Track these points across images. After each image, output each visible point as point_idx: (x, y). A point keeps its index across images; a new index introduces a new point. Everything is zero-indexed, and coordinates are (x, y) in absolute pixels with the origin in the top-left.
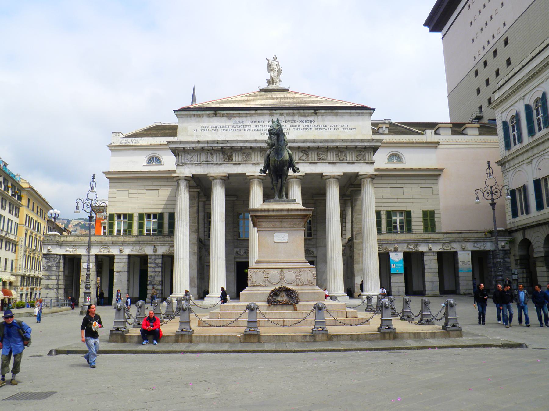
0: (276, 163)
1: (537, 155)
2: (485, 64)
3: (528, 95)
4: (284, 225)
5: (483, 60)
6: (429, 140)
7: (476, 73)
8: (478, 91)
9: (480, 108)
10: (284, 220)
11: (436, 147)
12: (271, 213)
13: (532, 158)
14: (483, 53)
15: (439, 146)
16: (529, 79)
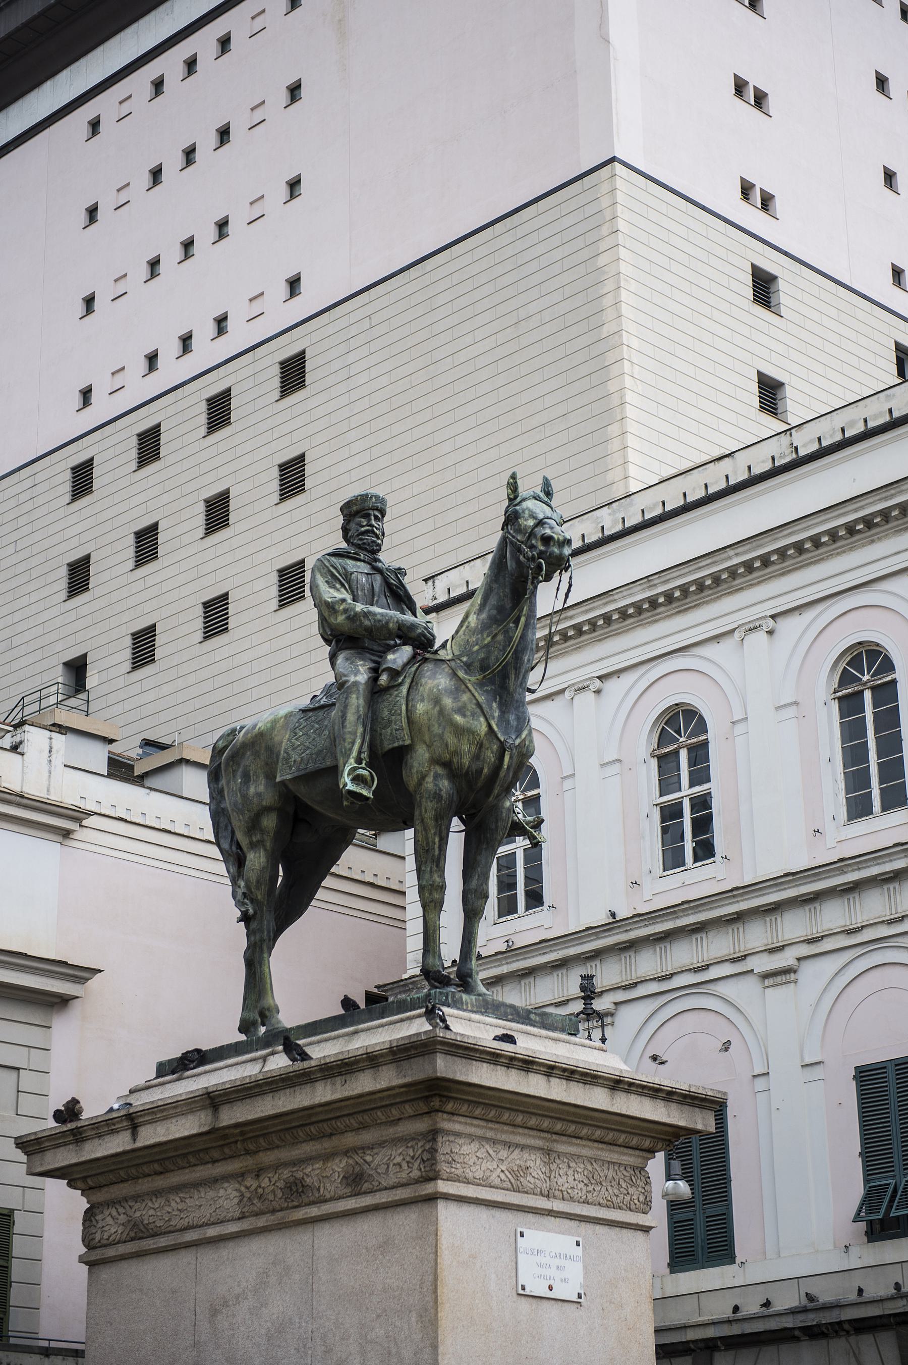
0: (490, 756)
1: (654, 988)
2: (149, 446)
3: (628, 679)
4: (569, 1178)
5: (143, 421)
6: (35, 789)
7: (82, 479)
8: (79, 576)
9: (77, 669)
10: (562, 1148)
11: (66, 834)
12: (535, 1086)
13: (621, 996)
14: (140, 387)
15: (81, 834)
16: (653, 603)
